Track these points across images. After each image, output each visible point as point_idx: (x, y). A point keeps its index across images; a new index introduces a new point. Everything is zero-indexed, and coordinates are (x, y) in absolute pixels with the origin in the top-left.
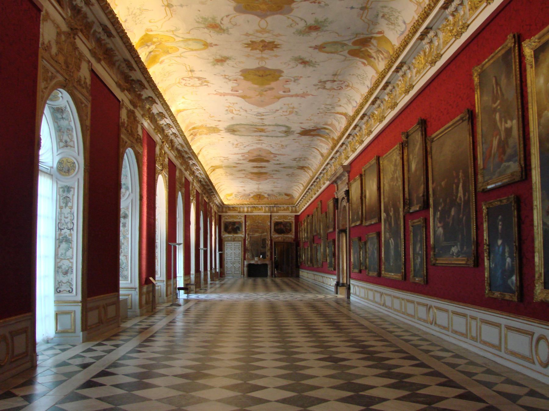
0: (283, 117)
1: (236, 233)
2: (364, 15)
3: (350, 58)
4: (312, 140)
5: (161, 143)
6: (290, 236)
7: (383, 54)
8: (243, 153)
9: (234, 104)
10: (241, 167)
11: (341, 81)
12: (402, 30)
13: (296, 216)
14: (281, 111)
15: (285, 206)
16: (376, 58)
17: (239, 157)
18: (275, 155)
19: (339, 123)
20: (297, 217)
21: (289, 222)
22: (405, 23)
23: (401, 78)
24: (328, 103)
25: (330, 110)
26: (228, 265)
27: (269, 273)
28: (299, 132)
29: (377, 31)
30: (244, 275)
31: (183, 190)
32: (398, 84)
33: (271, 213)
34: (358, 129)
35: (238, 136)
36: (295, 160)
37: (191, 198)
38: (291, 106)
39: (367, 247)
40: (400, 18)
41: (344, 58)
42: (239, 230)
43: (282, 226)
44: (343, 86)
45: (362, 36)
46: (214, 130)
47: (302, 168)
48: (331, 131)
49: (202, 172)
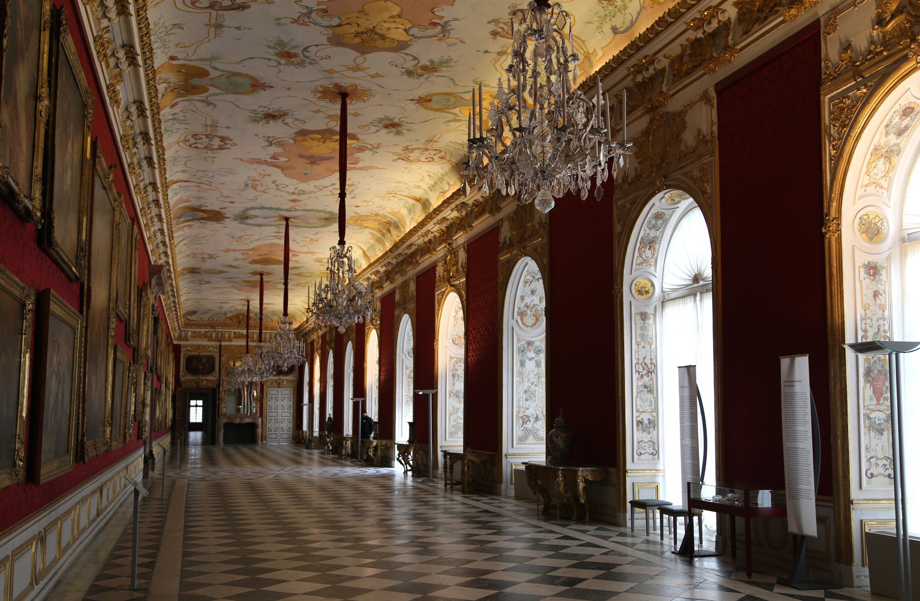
18: (273, 162)
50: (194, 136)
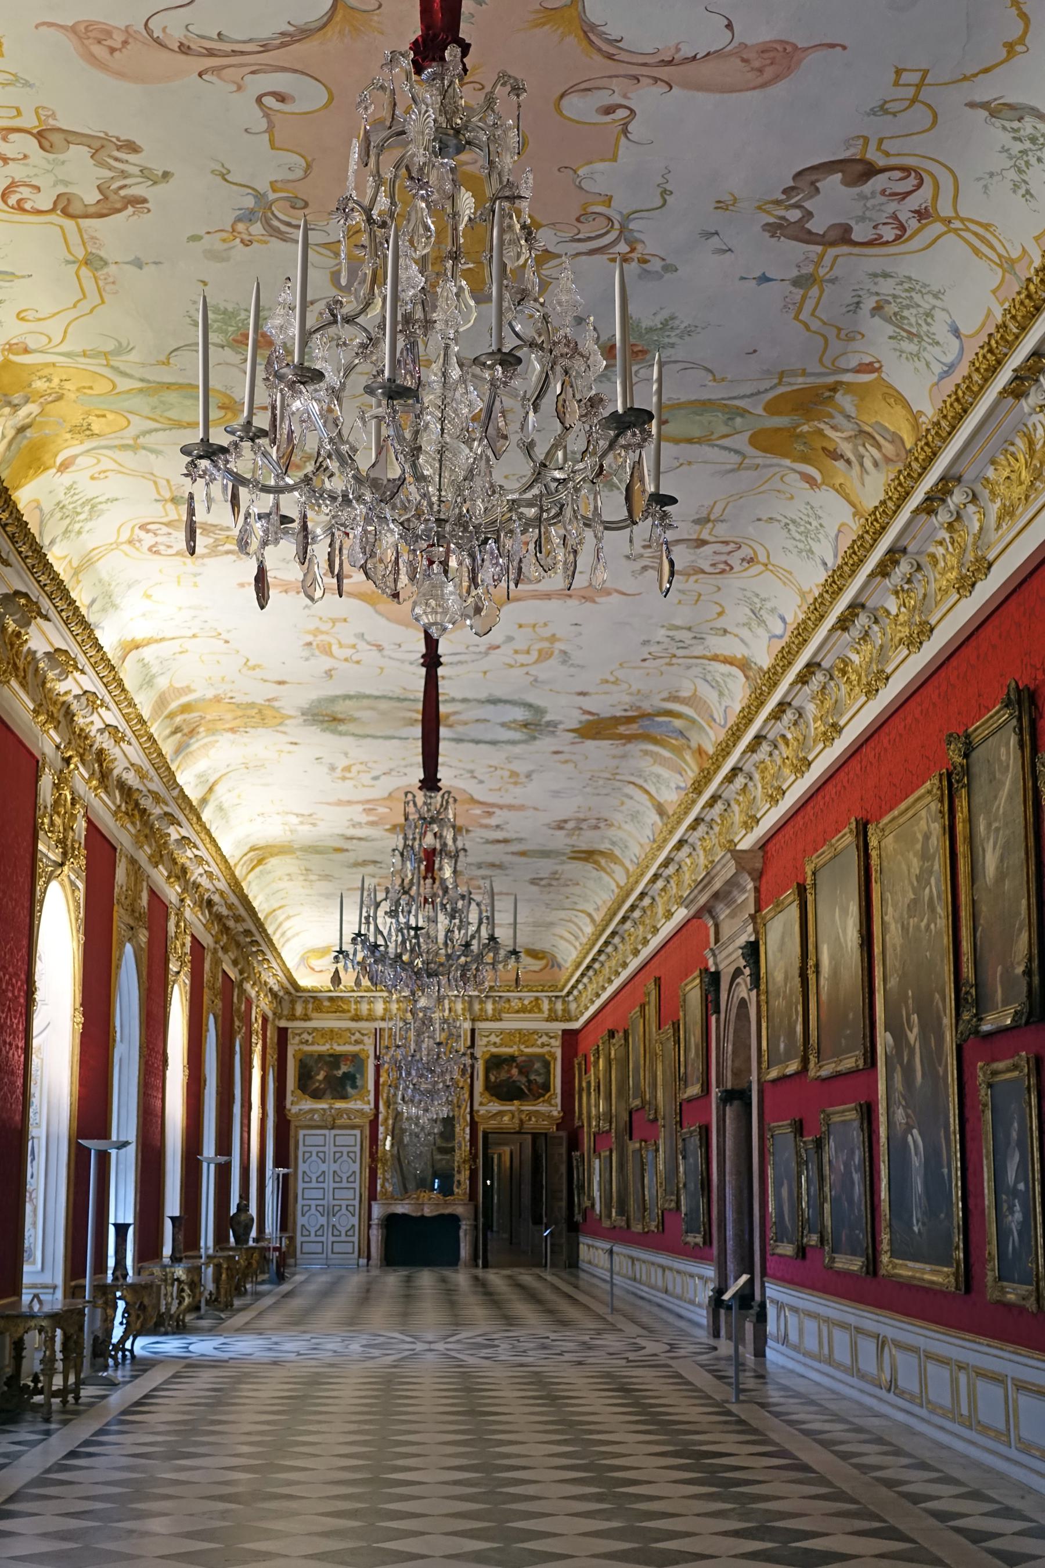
0: (520, 672)
1: (344, 1097)
2: (809, 305)
3: (759, 461)
4: (624, 756)
5: (59, 764)
6: (542, 1108)
7: (879, 447)
8: (368, 801)
9: (334, 621)
10: (363, 852)
11: (726, 543)
12: (949, 359)
13: (564, 1031)
14: (507, 649)
15: (528, 997)
16: (853, 458)
17: (357, 813)
18: (489, 810)
19: (721, 694)
20: (570, 1038)
21: (541, 1057)
22: (956, 332)
23: (944, 534)
24: (678, 622)
25: (685, 647)
26: (306, 1219)
27: (465, 1251)
28: (575, 725)
29: (853, 364)
30: (369, 1258)
31: (143, 937)
32: (933, 556)
33: (473, 1020)
34: (789, 716)
35: (350, 739)
36: (560, 826)
37: (173, 967)
38: (546, 633)
39: (826, 1160)
40: (938, 314)
41: (736, 459)
42: (354, 1086)
43: (515, 1071)
44: (734, 560)
45: (800, 380)
46: (259, 715)
47: (588, 856)
48: (693, 721)
49: (214, 869)
50: (597, 827)
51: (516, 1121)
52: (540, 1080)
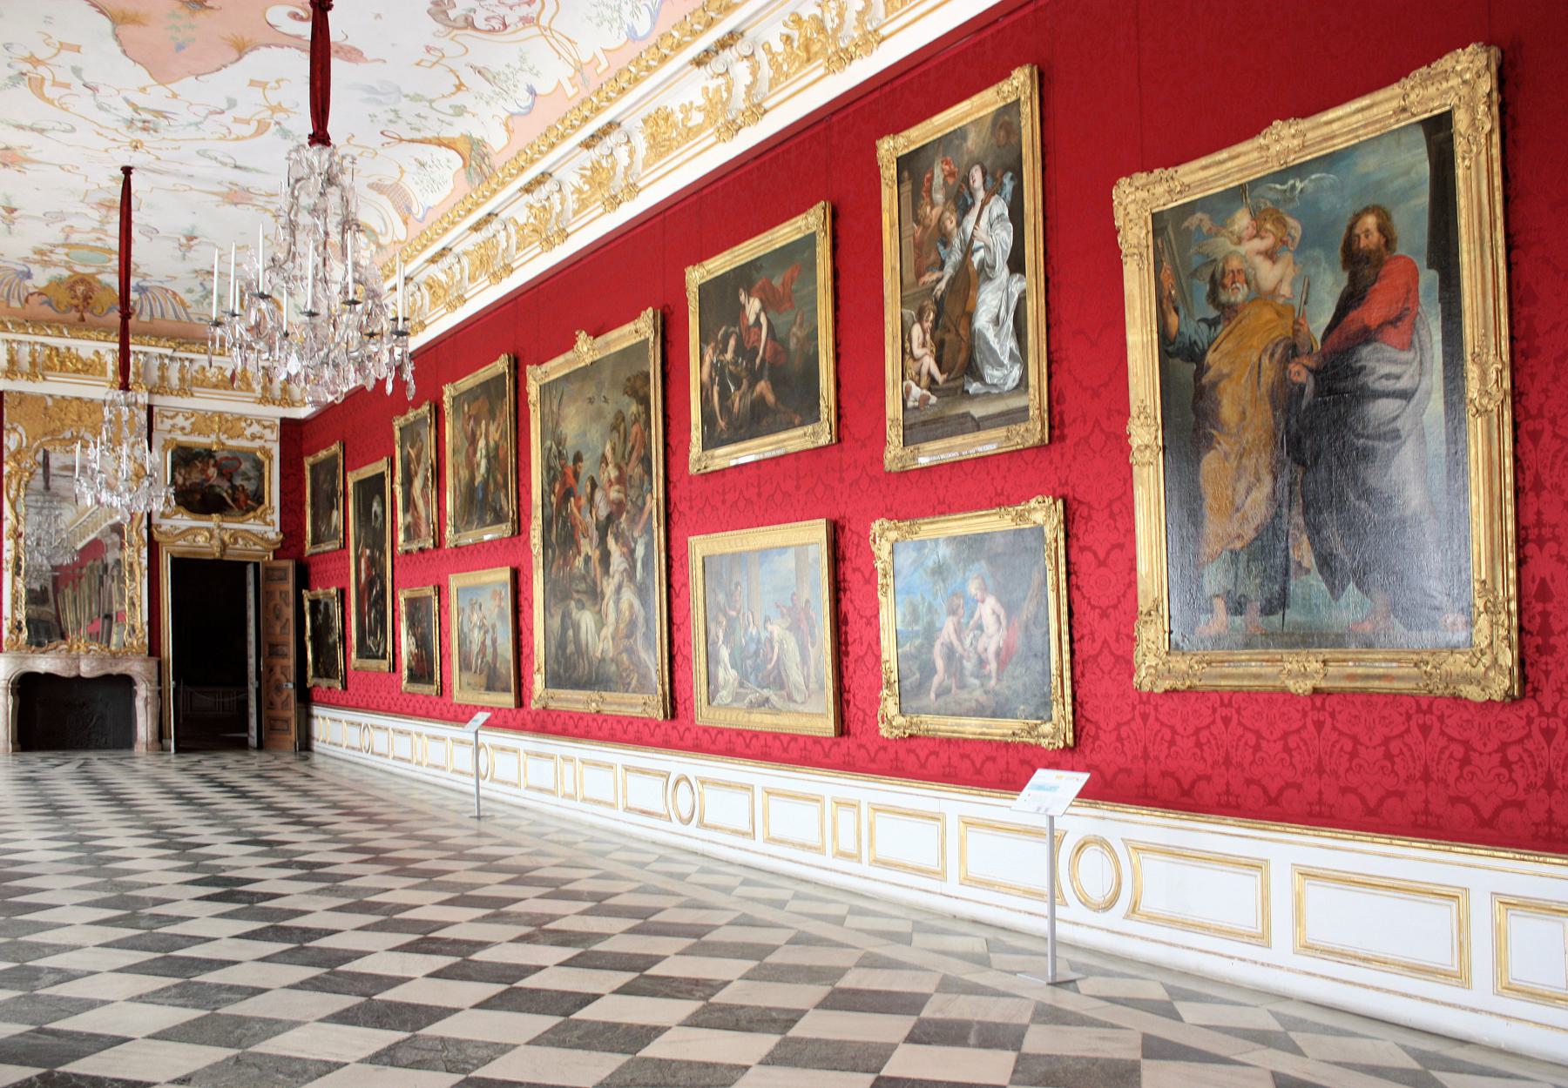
6: (252, 525)
13: (285, 422)
21: (250, 455)
33: (151, 392)
43: (212, 471)
51: (216, 543)
52: (250, 487)
